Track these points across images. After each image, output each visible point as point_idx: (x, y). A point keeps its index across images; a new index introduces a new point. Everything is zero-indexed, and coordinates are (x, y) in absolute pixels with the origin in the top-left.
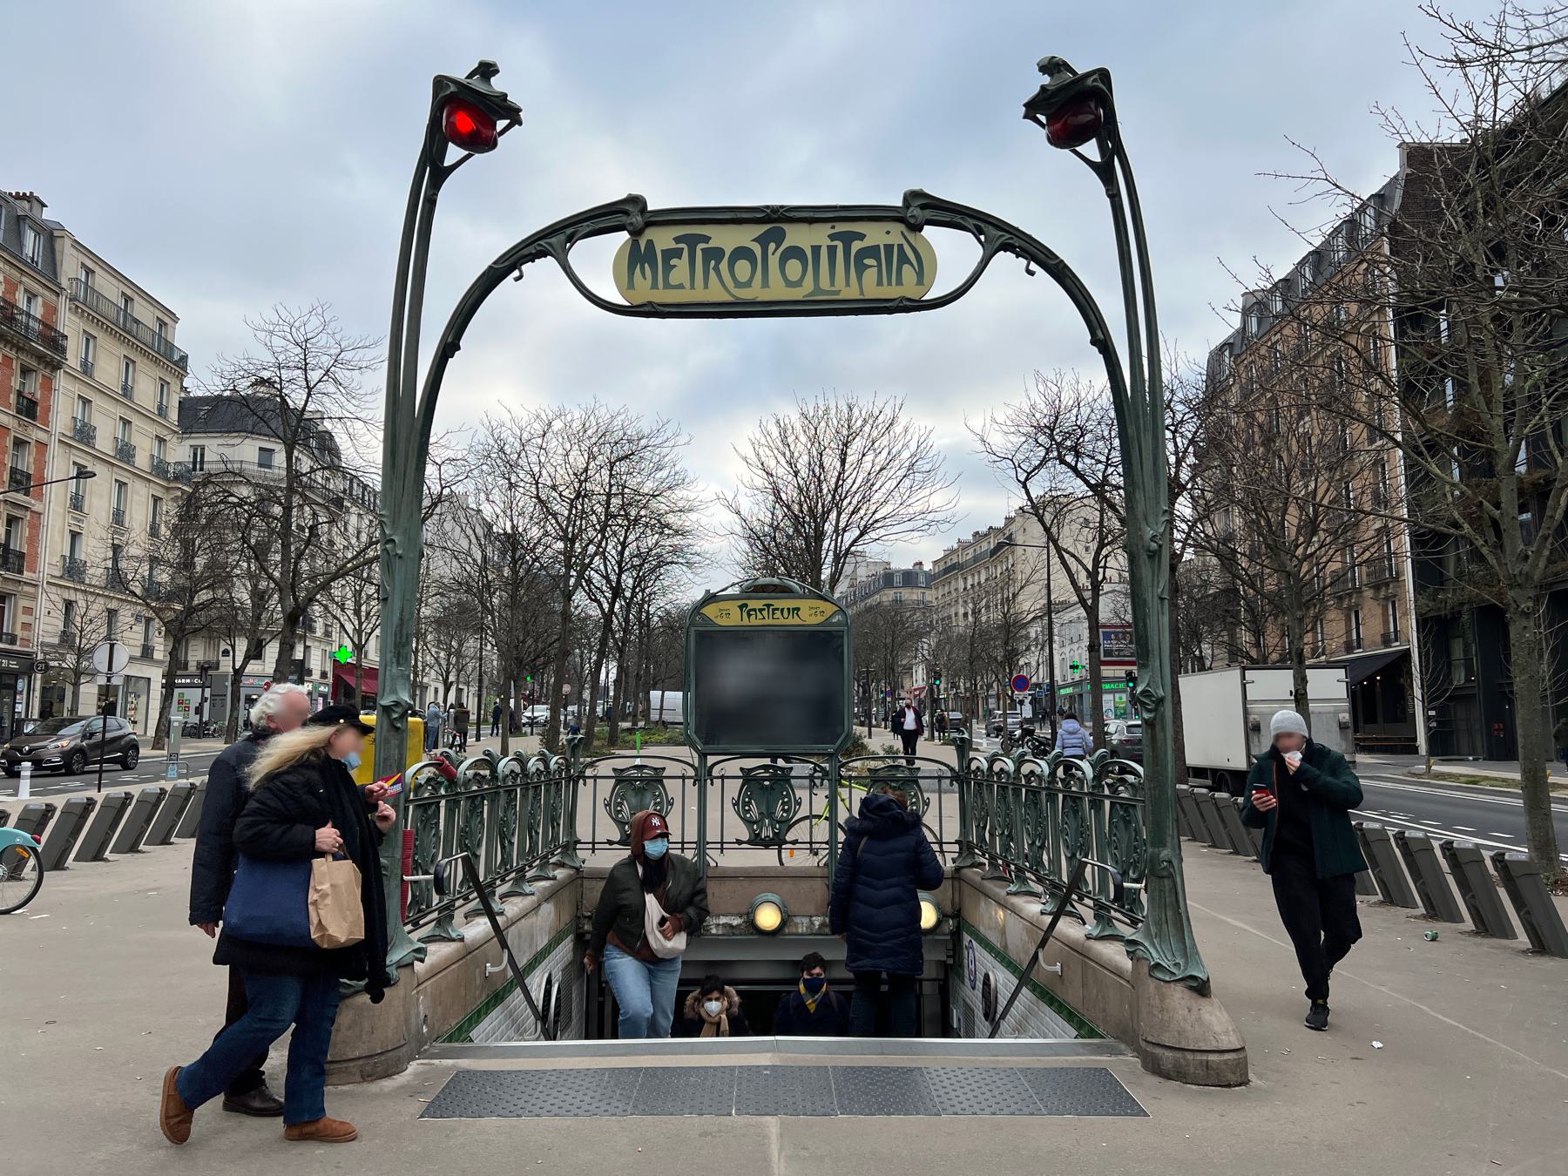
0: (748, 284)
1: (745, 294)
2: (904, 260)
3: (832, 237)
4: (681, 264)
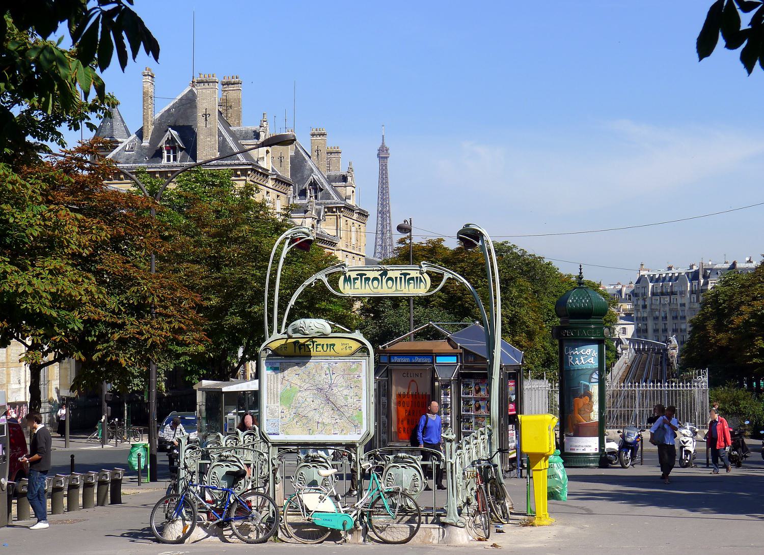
0: (377, 288)
1: (375, 290)
2: (421, 281)
3: (401, 274)
4: (358, 282)
